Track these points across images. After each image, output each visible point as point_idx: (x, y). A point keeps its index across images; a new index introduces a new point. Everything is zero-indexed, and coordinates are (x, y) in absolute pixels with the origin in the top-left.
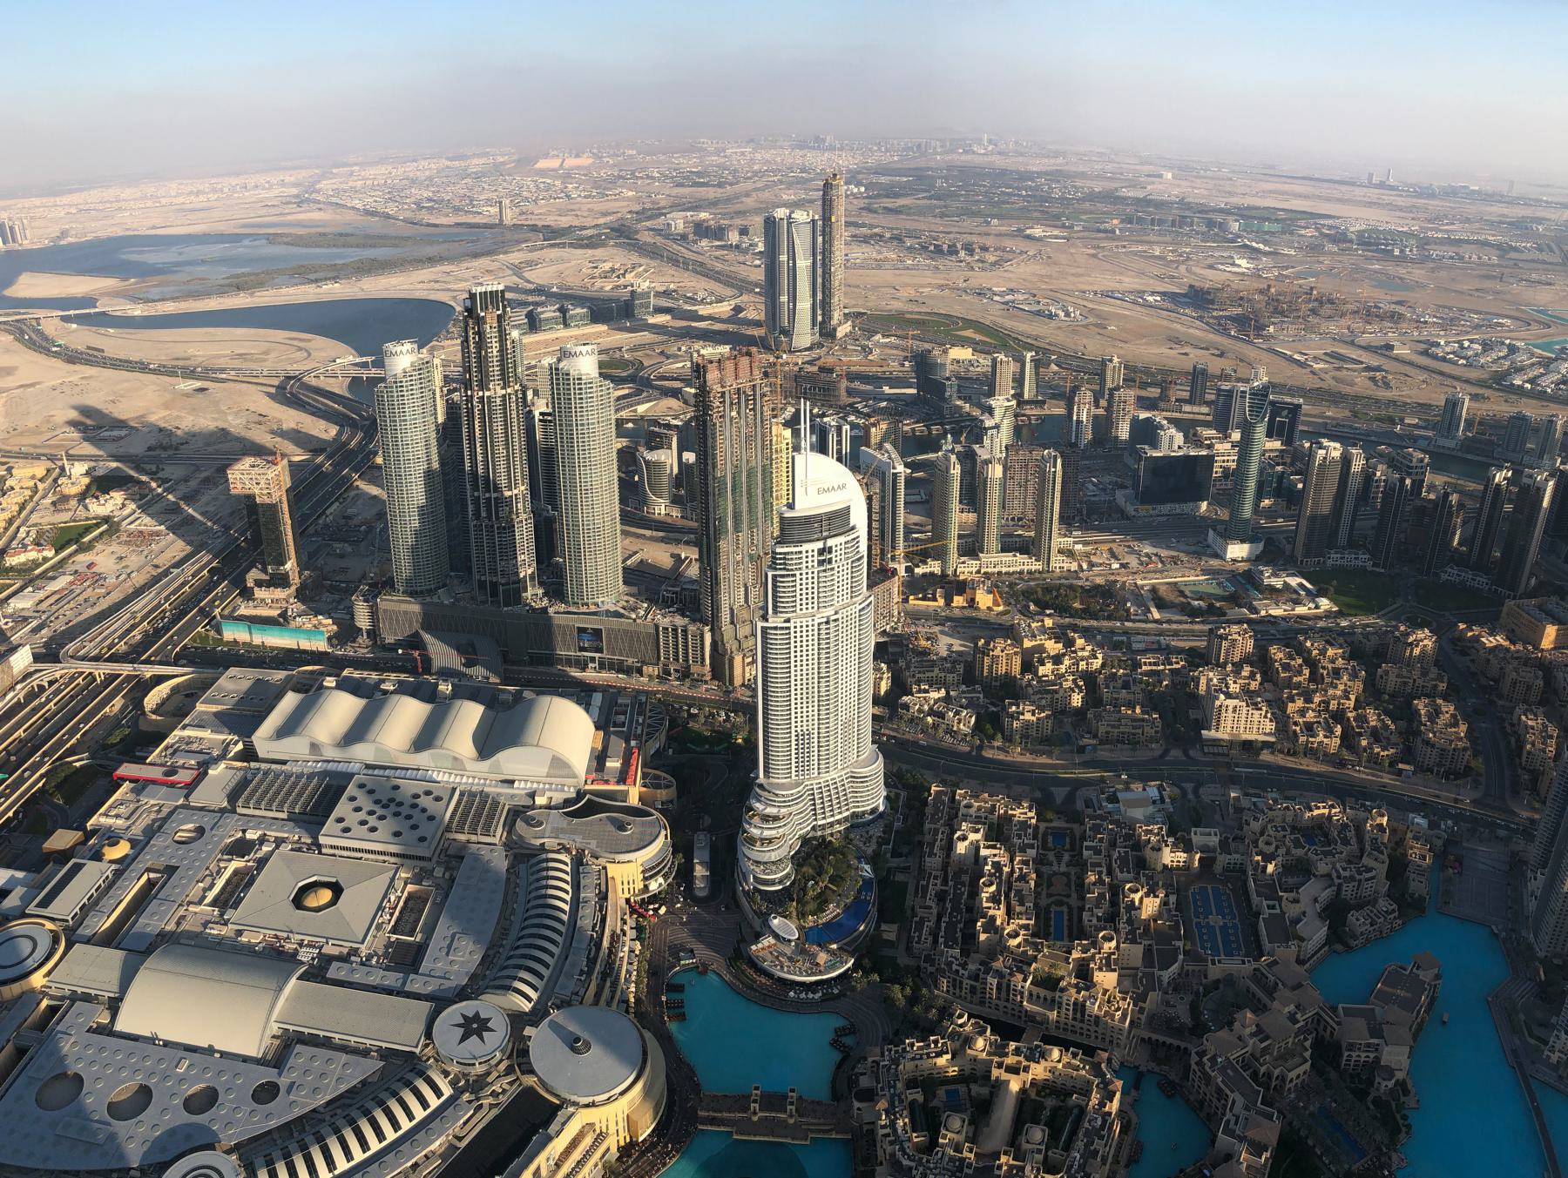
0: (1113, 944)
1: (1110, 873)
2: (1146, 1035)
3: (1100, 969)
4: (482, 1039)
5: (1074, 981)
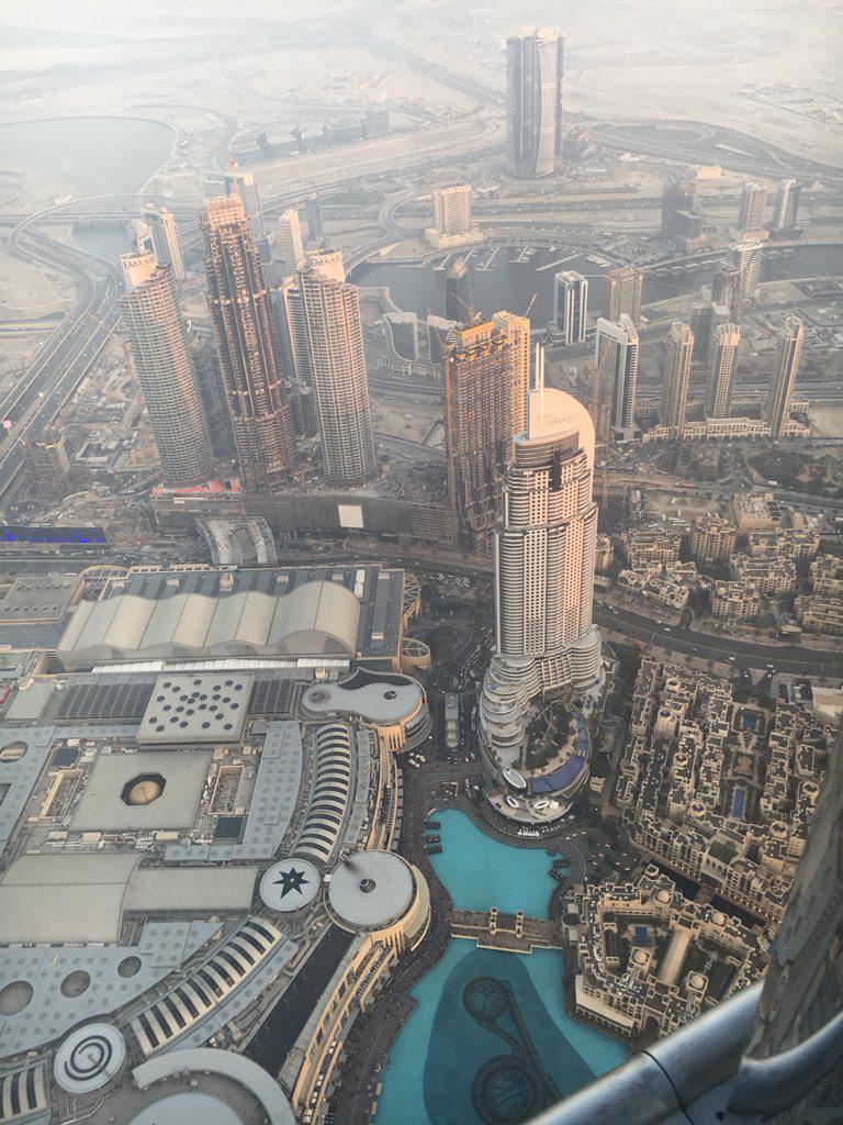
0: (784, 834)
1: (792, 765)
3: (768, 854)
4: (299, 890)
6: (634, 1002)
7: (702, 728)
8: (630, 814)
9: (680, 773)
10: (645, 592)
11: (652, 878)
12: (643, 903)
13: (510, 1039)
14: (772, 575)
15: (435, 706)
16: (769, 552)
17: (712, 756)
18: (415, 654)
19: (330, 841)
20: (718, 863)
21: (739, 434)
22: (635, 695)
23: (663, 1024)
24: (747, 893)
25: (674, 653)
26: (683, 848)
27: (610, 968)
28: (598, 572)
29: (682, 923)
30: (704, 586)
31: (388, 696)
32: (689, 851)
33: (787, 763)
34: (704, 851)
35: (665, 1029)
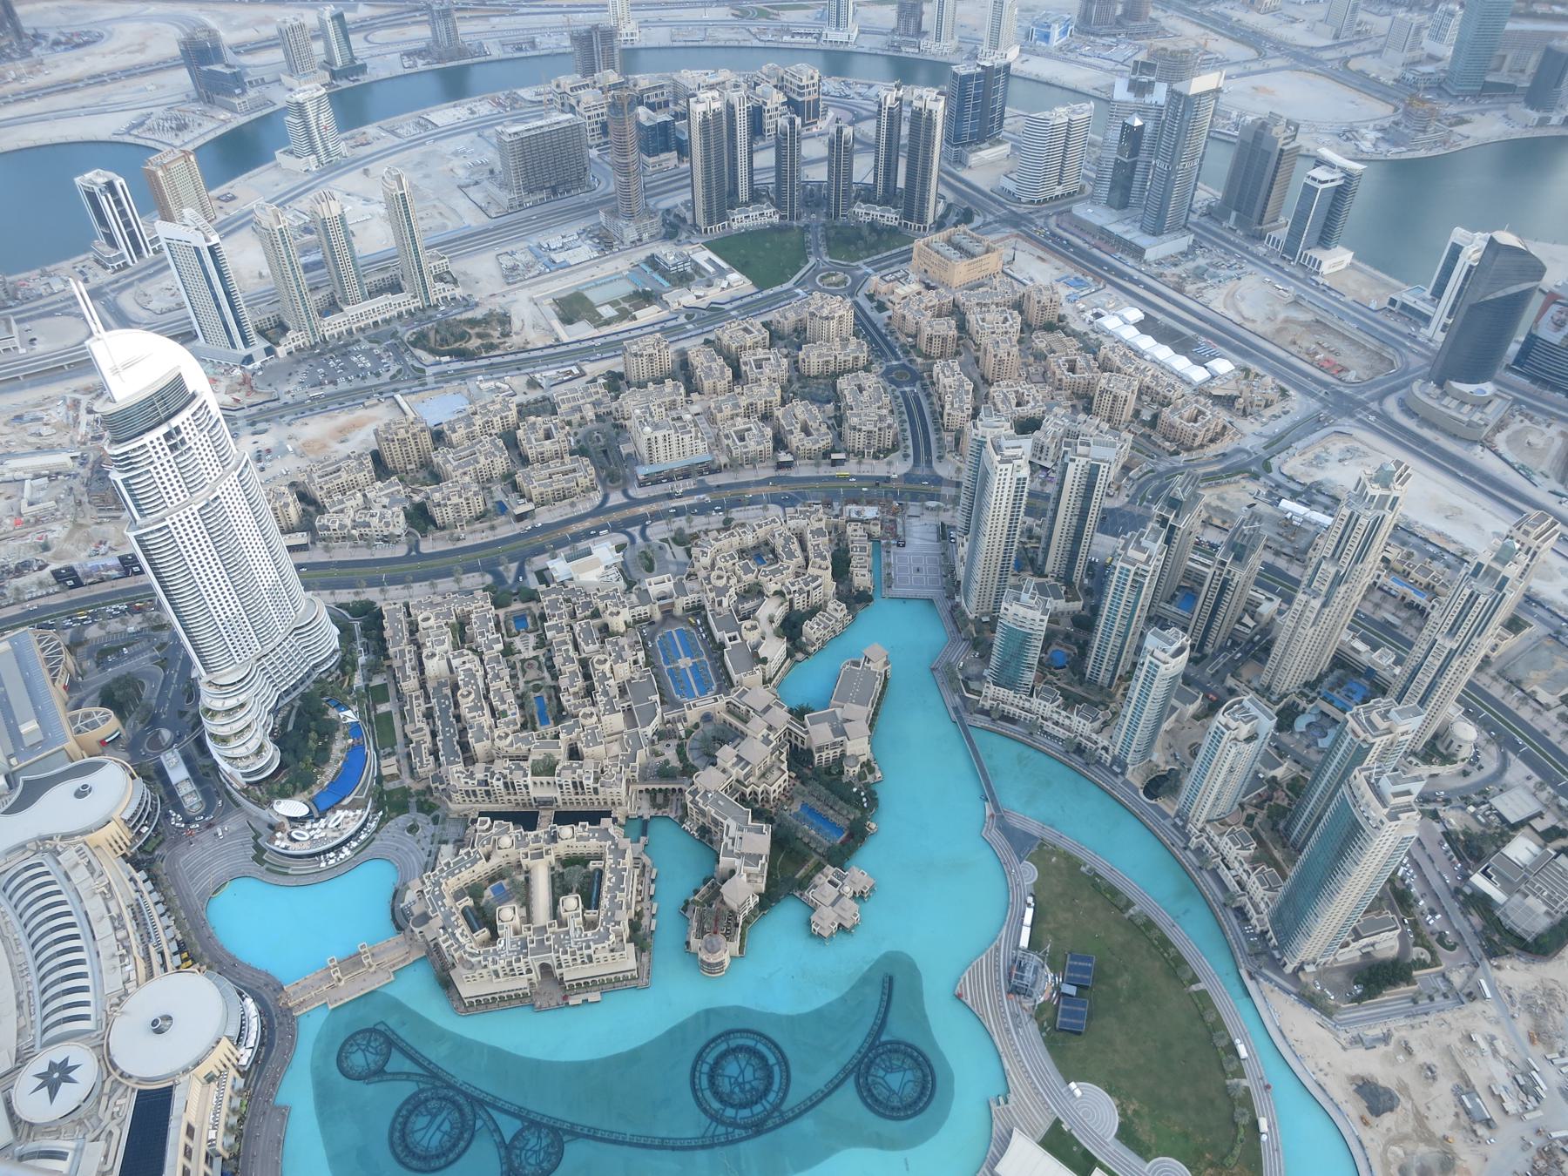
0: (595, 718)
1: (576, 647)
2: (643, 787)
3: (588, 746)
4: (72, 1081)
5: (567, 763)
6: (518, 960)
7: (475, 651)
8: (438, 778)
9: (471, 710)
11: (488, 830)
12: (488, 859)
13: (408, 1076)
14: (482, 459)
15: (155, 776)
16: (471, 437)
17: (497, 676)
18: (94, 725)
19: (86, 1004)
20: (545, 779)
21: (387, 316)
22: (391, 651)
26: (506, 784)
27: (485, 944)
29: (534, 857)
30: (417, 499)
31: (81, 793)
33: (571, 647)
34: (526, 775)
35: (560, 966)
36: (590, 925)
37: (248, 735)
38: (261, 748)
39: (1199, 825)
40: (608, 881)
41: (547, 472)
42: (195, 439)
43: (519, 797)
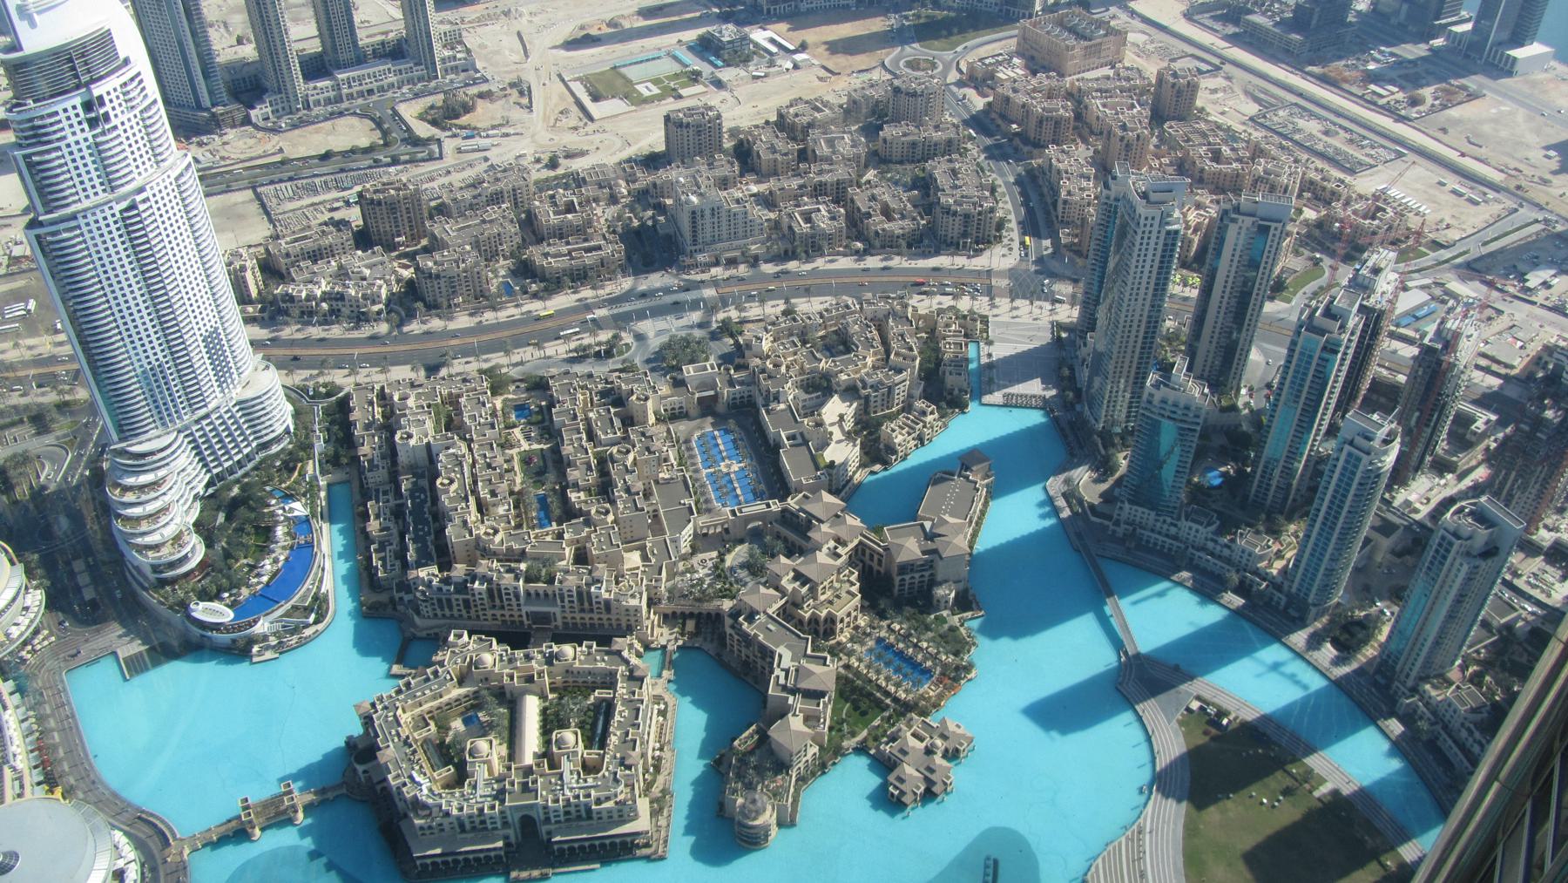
0: (610, 518)
1: (591, 436)
10: (325, 305)
23: (542, 817)
24: (592, 611)
25: (393, 368)
26: (490, 591)
28: (243, 298)
32: (499, 590)
34: (517, 579)
35: (547, 820)
36: (589, 768)
37: (164, 520)
38: (177, 539)
39: (1410, 683)
40: (621, 713)
41: (564, 249)
42: (120, 116)
43: (507, 613)
